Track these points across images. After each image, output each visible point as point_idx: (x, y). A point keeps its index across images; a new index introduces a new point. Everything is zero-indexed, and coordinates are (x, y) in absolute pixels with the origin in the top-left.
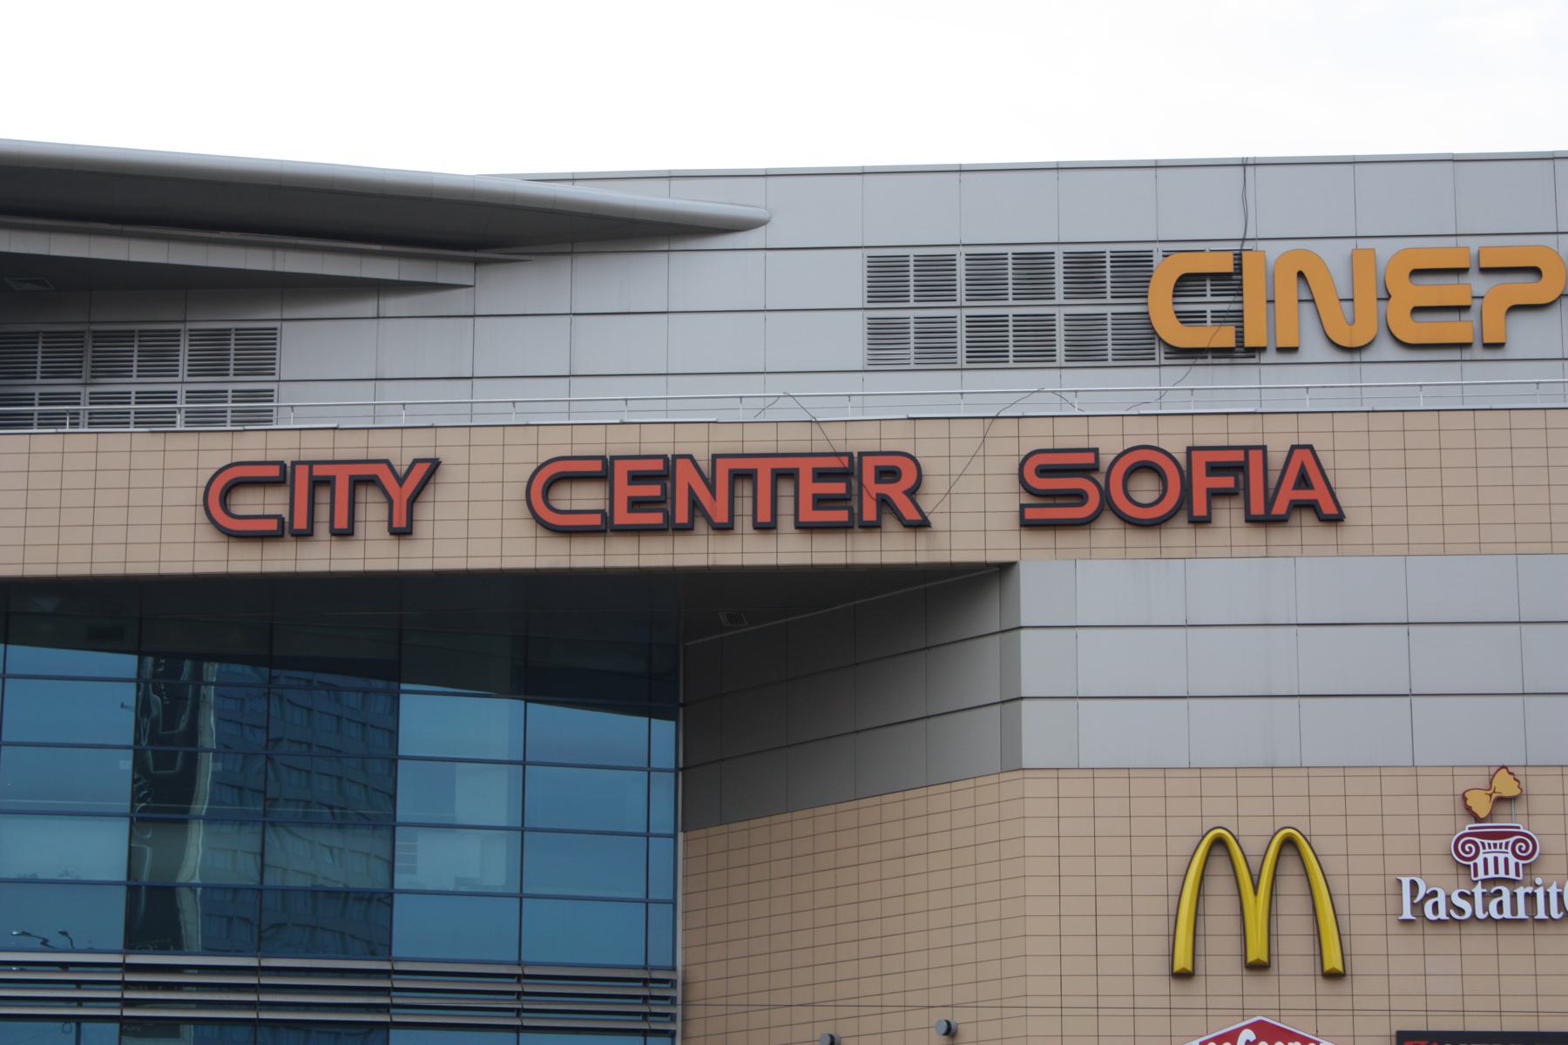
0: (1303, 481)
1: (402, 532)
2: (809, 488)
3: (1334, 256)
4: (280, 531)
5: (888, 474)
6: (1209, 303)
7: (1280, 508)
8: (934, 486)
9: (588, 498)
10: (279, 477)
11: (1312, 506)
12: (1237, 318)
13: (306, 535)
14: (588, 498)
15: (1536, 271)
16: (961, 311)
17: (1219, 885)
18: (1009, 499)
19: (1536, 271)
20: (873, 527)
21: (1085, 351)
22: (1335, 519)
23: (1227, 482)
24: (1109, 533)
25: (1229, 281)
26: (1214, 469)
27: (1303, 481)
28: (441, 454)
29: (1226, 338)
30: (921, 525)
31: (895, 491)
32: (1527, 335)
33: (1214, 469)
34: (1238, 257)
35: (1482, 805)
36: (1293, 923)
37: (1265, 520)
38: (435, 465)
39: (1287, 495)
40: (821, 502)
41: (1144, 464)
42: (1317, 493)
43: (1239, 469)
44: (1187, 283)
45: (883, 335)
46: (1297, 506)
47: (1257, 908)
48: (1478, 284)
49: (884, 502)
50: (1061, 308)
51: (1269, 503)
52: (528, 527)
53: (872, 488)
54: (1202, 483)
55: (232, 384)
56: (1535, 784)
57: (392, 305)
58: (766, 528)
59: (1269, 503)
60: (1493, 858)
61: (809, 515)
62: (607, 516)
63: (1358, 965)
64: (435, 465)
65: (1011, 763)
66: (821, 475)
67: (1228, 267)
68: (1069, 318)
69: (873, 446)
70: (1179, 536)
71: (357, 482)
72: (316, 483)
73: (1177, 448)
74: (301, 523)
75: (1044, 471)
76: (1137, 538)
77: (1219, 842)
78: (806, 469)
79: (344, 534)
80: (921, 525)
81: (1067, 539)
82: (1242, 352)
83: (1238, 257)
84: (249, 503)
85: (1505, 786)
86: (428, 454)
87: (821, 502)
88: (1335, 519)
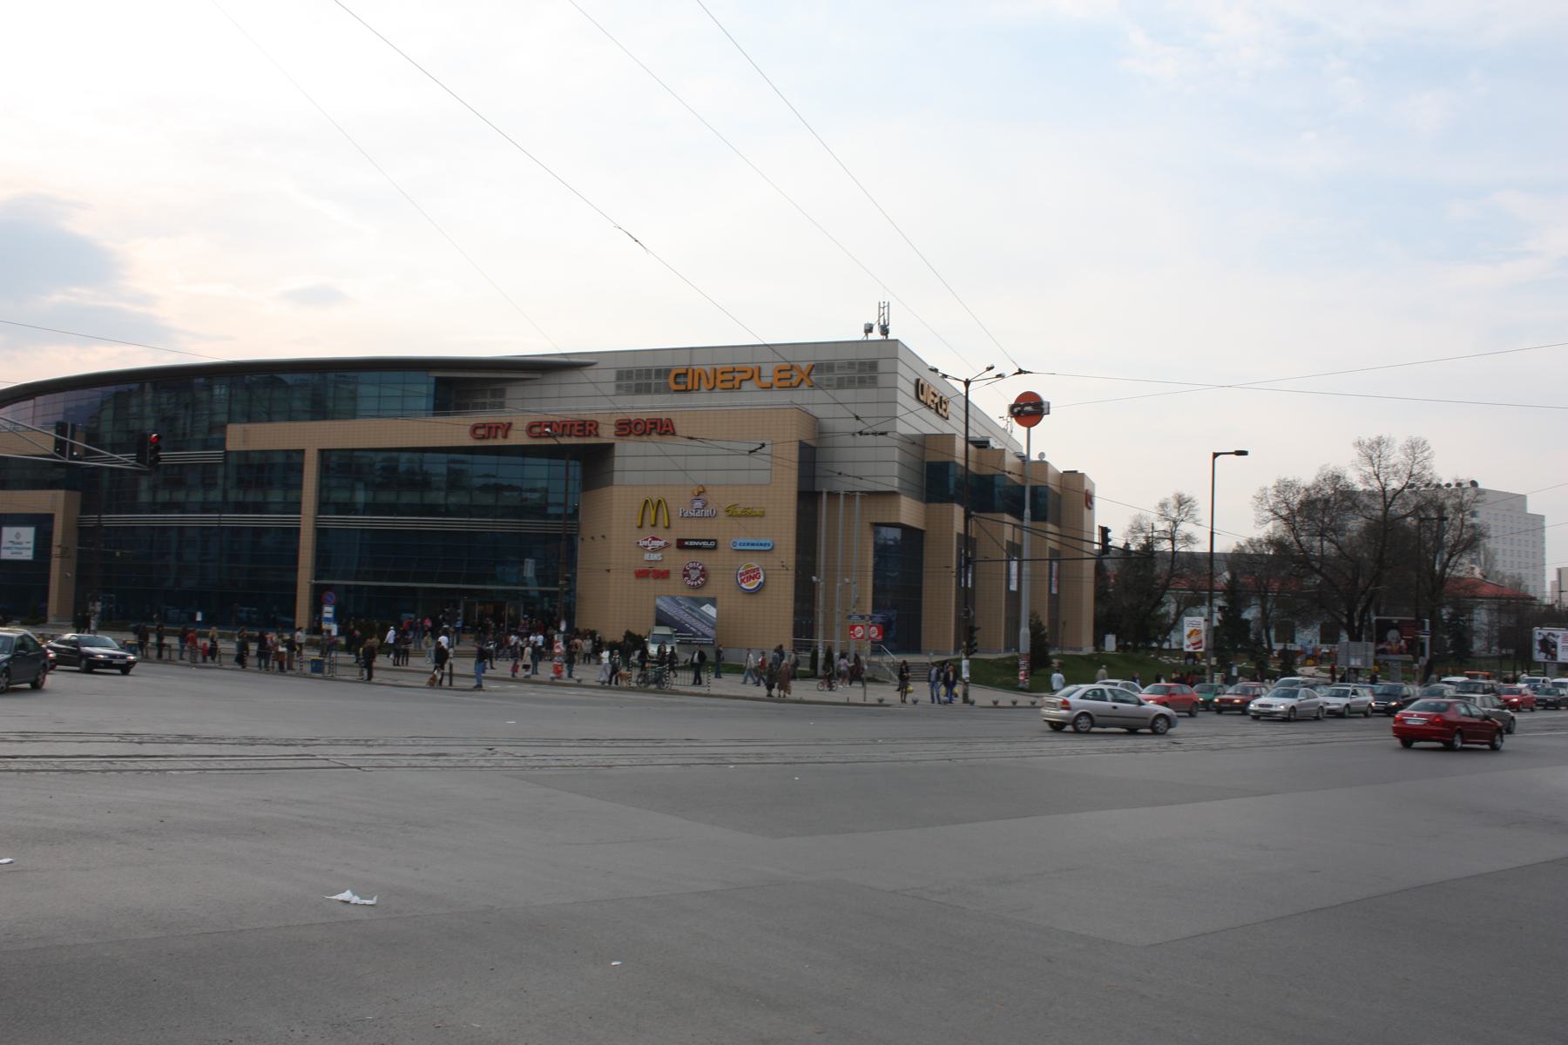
0: (667, 426)
1: (505, 437)
2: (576, 428)
3: (707, 368)
4: (484, 437)
5: (591, 425)
6: (680, 380)
7: (662, 432)
8: (601, 426)
9: (537, 430)
10: (484, 426)
11: (668, 431)
12: (685, 383)
13: (488, 438)
14: (537, 430)
15: (746, 372)
16: (633, 383)
17: (647, 509)
18: (613, 429)
19: (746, 372)
20: (589, 435)
21: (658, 391)
22: (674, 434)
23: (653, 426)
24: (632, 437)
25: (686, 374)
26: (651, 423)
27: (667, 426)
28: (513, 421)
29: (683, 387)
30: (597, 435)
31: (592, 428)
32: (746, 386)
33: (651, 423)
34: (687, 370)
35: (696, 493)
36: (660, 517)
37: (660, 434)
38: (510, 424)
39: (664, 429)
40: (579, 431)
41: (637, 423)
42: (670, 428)
43: (655, 424)
44: (677, 376)
45: (618, 387)
46: (666, 431)
47: (653, 513)
48: (736, 375)
49: (590, 431)
50: (654, 381)
51: (661, 429)
52: (527, 437)
53: (588, 428)
54: (649, 426)
55: (498, 400)
56: (707, 489)
57: (528, 382)
58: (570, 435)
59: (661, 429)
60: (698, 504)
61: (577, 434)
62: (540, 434)
63: (672, 525)
64: (510, 424)
65: (611, 483)
66: (579, 425)
67: (684, 372)
68: (656, 383)
69: (590, 419)
70: (645, 438)
71: (497, 428)
72: (490, 428)
73: (645, 419)
74: (487, 436)
75: (620, 424)
76: (638, 438)
77: (647, 502)
78: (576, 424)
79: (495, 437)
80: (597, 435)
81: (625, 438)
82: (686, 391)
83: (687, 370)
84: (481, 432)
85: (701, 490)
86: (509, 421)
87: (579, 431)
88: (674, 434)
